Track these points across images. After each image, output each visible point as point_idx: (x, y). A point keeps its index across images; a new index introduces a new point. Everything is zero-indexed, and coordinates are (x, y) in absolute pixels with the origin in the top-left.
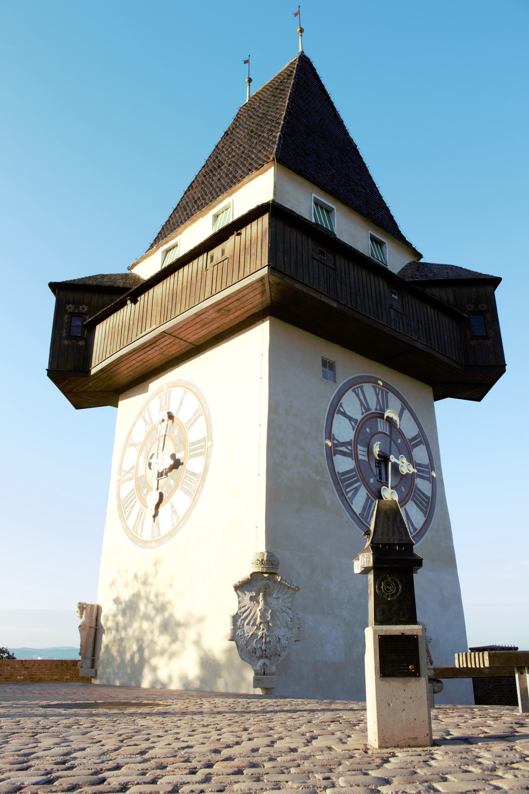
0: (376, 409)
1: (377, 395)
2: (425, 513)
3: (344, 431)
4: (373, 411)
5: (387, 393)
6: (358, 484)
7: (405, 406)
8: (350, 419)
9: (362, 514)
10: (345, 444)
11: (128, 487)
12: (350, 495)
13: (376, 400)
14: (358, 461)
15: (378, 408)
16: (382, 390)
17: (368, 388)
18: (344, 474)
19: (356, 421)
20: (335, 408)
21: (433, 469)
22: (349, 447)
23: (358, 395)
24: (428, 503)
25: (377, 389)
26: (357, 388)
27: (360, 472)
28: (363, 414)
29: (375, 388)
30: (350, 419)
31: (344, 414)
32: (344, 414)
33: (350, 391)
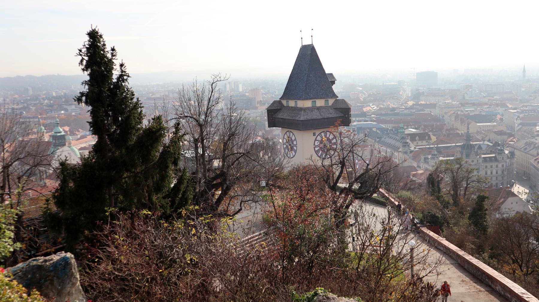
20: (316, 140)
27: (321, 148)
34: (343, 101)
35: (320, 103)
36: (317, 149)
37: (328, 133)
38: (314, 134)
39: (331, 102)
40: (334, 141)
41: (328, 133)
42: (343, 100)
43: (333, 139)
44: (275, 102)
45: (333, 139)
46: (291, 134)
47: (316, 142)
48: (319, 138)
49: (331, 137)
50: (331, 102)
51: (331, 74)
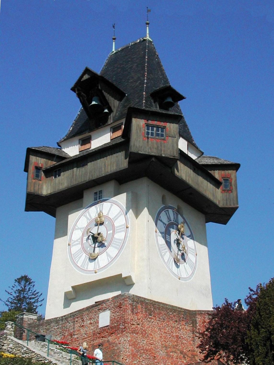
0: (173, 221)
1: (174, 215)
4: (172, 221)
5: (178, 215)
6: (166, 250)
7: (185, 222)
8: (164, 223)
12: (163, 254)
15: (174, 220)
16: (176, 213)
17: (170, 211)
18: (161, 245)
19: (166, 224)
22: (163, 234)
23: (166, 214)
24: (193, 266)
25: (174, 212)
26: (166, 210)
28: (168, 222)
30: (164, 223)
31: (161, 221)
32: (161, 221)
33: (163, 211)
47: (159, 222)
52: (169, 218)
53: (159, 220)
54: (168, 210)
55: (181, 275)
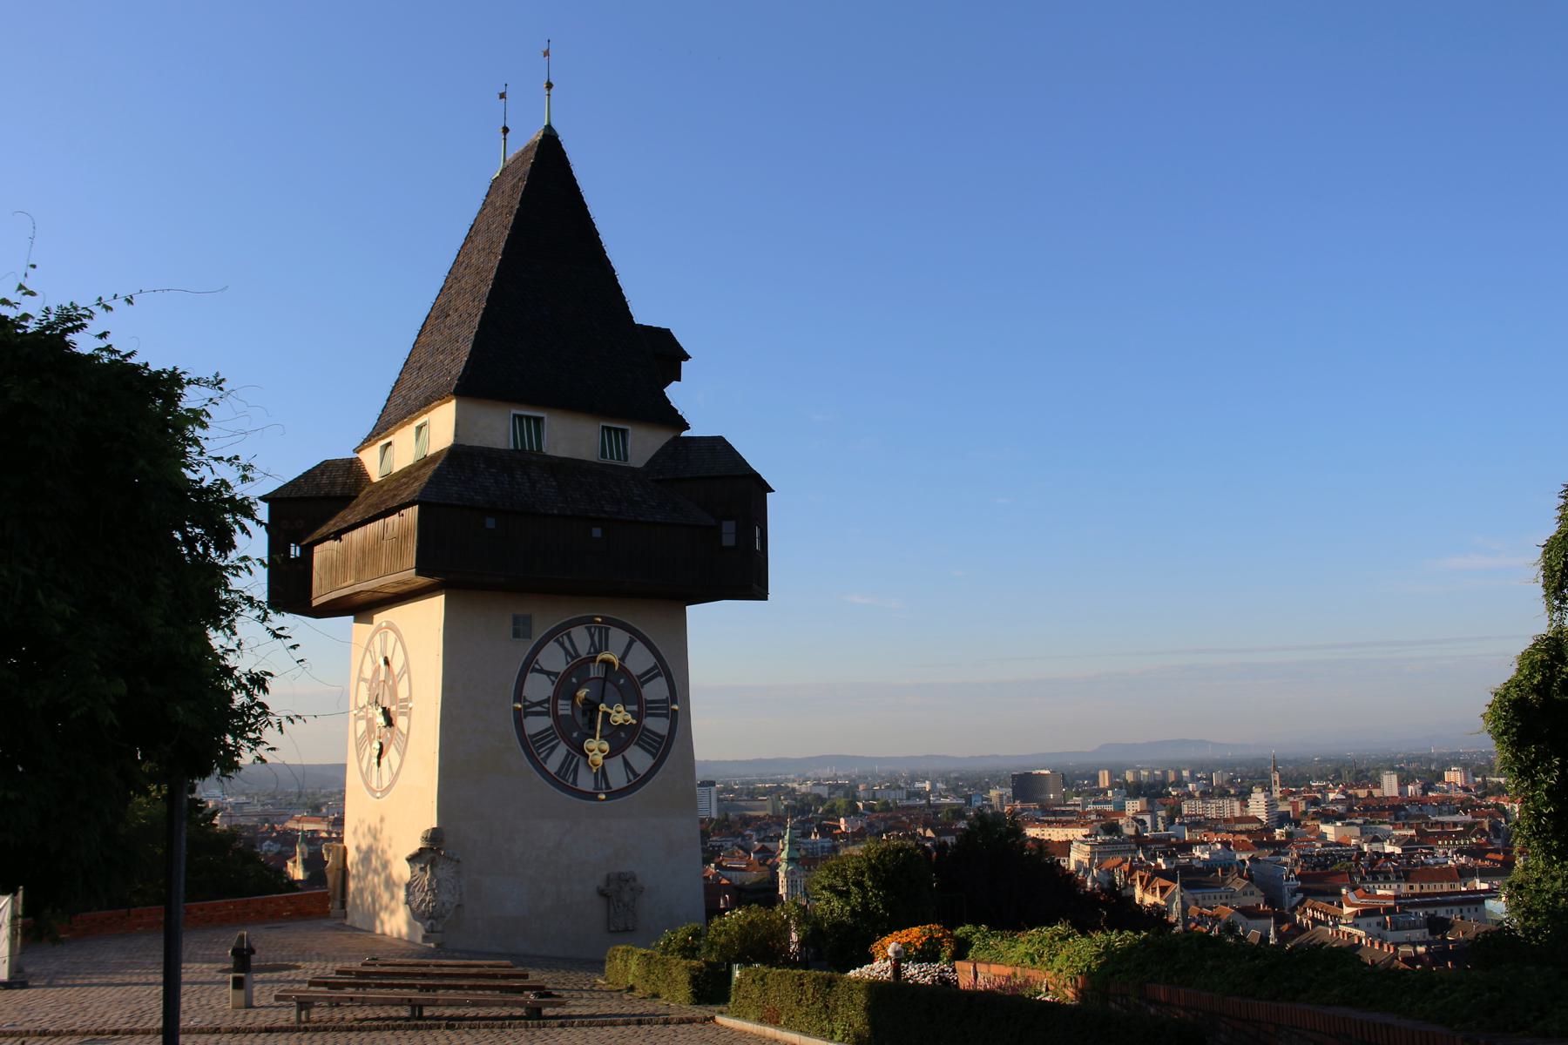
1: (592, 636)
2: (654, 756)
3: (538, 688)
7: (636, 635)
8: (548, 673)
9: (558, 773)
10: (540, 703)
11: (362, 725)
13: (588, 642)
14: (557, 717)
19: (556, 674)
20: (529, 666)
21: (674, 701)
29: (589, 629)
30: (548, 673)
31: (542, 671)
34: (718, 447)
35: (570, 437)
36: (535, 725)
37: (618, 638)
38: (521, 630)
39: (643, 444)
40: (655, 690)
41: (618, 638)
42: (721, 440)
43: (649, 676)
44: (326, 466)
45: (649, 676)
46: (392, 636)
48: (554, 659)
49: (640, 660)
50: (643, 444)
51: (664, 336)
52: (572, 654)
53: (535, 670)
54: (569, 635)
55: (608, 787)
